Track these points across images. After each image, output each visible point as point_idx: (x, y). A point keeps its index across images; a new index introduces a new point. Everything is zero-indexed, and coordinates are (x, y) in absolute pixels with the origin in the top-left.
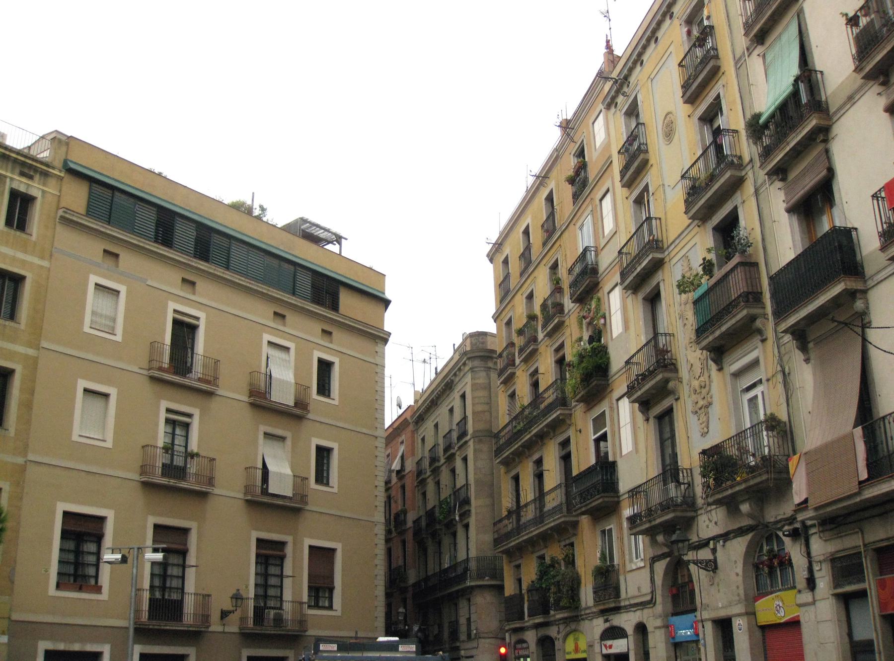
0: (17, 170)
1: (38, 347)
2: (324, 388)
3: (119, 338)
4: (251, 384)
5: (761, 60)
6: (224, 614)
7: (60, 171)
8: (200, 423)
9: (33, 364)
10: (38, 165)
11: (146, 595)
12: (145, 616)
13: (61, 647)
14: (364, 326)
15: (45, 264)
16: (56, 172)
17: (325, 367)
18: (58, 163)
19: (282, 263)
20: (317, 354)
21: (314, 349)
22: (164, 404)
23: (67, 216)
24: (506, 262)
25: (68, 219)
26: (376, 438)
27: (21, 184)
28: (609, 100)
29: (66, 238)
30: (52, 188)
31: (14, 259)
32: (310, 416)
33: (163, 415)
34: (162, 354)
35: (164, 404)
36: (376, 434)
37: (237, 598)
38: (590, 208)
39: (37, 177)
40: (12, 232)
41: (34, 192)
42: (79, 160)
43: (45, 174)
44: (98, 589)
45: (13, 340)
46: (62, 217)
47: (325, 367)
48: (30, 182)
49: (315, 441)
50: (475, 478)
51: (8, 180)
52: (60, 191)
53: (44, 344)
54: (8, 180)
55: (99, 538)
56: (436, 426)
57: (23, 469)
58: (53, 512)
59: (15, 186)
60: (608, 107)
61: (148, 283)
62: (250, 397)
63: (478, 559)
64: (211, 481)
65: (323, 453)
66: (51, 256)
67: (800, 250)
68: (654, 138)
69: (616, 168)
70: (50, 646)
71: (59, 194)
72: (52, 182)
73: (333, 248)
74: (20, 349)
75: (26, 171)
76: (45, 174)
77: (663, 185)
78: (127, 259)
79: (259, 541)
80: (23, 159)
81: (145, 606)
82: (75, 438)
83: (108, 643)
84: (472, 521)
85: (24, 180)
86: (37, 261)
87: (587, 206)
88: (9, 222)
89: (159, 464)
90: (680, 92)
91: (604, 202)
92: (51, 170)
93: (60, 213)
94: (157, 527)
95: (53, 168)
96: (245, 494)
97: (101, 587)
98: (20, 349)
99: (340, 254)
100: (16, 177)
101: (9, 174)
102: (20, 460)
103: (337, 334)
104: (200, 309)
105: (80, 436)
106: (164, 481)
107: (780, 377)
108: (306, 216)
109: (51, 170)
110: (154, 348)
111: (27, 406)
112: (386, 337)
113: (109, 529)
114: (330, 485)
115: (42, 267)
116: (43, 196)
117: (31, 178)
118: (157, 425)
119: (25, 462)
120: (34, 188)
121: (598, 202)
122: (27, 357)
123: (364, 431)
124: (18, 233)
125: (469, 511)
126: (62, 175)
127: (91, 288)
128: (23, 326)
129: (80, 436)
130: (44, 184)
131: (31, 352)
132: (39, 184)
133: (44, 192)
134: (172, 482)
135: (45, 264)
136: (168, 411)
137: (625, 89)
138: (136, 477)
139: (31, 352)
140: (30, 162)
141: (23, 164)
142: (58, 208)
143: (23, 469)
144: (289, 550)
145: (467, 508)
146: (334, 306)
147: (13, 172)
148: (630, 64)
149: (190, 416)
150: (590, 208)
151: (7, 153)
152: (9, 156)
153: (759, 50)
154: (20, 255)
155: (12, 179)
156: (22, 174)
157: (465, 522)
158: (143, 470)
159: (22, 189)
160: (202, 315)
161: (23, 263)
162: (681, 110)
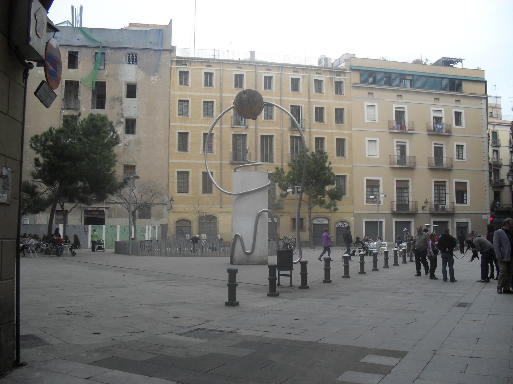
0: (336, 75)
1: (351, 130)
2: (458, 121)
3: (377, 121)
4: (427, 127)
6: (423, 208)
7: (349, 70)
8: (409, 144)
9: (350, 136)
10: (342, 71)
11: (395, 203)
12: (395, 210)
13: (370, 220)
14: (474, 95)
15: (350, 103)
16: (348, 71)
17: (458, 115)
18: (348, 68)
19: (436, 79)
20: (454, 110)
21: (452, 109)
22: (395, 140)
23: (354, 85)
25: (354, 86)
26: (483, 138)
27: (337, 78)
29: (355, 93)
30: (348, 77)
32: (452, 134)
33: (395, 144)
34: (393, 123)
35: (395, 140)
36: (483, 136)
37: (426, 202)
39: (342, 75)
41: (342, 81)
42: (355, 64)
43: (345, 73)
46: (352, 86)
47: (458, 115)
48: (340, 77)
49: (456, 143)
51: (333, 79)
52: (350, 77)
53: (353, 129)
54: (333, 79)
55: (378, 187)
57: (352, 168)
58: (363, 180)
62: (427, 132)
64: (415, 164)
65: (460, 147)
66: (351, 100)
70: (366, 220)
71: (350, 78)
72: (347, 75)
73: (458, 65)
74: (346, 132)
75: (338, 74)
76: (345, 73)
78: (376, 94)
79: (435, 182)
80: (336, 70)
81: (395, 207)
82: (367, 156)
83: (384, 218)
85: (338, 77)
86: (347, 102)
88: (336, 93)
89: (396, 161)
92: (346, 71)
93: (351, 85)
94: (397, 181)
95: (347, 70)
96: (428, 166)
97: (380, 201)
98: (346, 132)
99: (462, 68)
100: (336, 77)
101: (333, 77)
102: (351, 166)
103: (463, 101)
104: (405, 105)
106: (398, 166)
108: (445, 56)
110: (390, 122)
111: (351, 149)
113: (381, 183)
115: (349, 104)
116: (345, 81)
117: (340, 76)
118: (393, 147)
119: (353, 166)
120: (342, 78)
123: (477, 136)
124: (340, 95)
126: (350, 72)
127: (365, 106)
128: (346, 125)
130: (345, 77)
131: (350, 132)
133: (345, 79)
134: (401, 166)
135: (350, 103)
138: (389, 166)
139: (350, 132)
140: (339, 71)
141: (337, 72)
142: (351, 83)
143: (352, 168)
144: (447, 184)
147: (334, 76)
151: (332, 70)
154: (342, 102)
155: (334, 78)
156: (337, 75)
158: (391, 163)
159: (338, 80)
160: (406, 106)
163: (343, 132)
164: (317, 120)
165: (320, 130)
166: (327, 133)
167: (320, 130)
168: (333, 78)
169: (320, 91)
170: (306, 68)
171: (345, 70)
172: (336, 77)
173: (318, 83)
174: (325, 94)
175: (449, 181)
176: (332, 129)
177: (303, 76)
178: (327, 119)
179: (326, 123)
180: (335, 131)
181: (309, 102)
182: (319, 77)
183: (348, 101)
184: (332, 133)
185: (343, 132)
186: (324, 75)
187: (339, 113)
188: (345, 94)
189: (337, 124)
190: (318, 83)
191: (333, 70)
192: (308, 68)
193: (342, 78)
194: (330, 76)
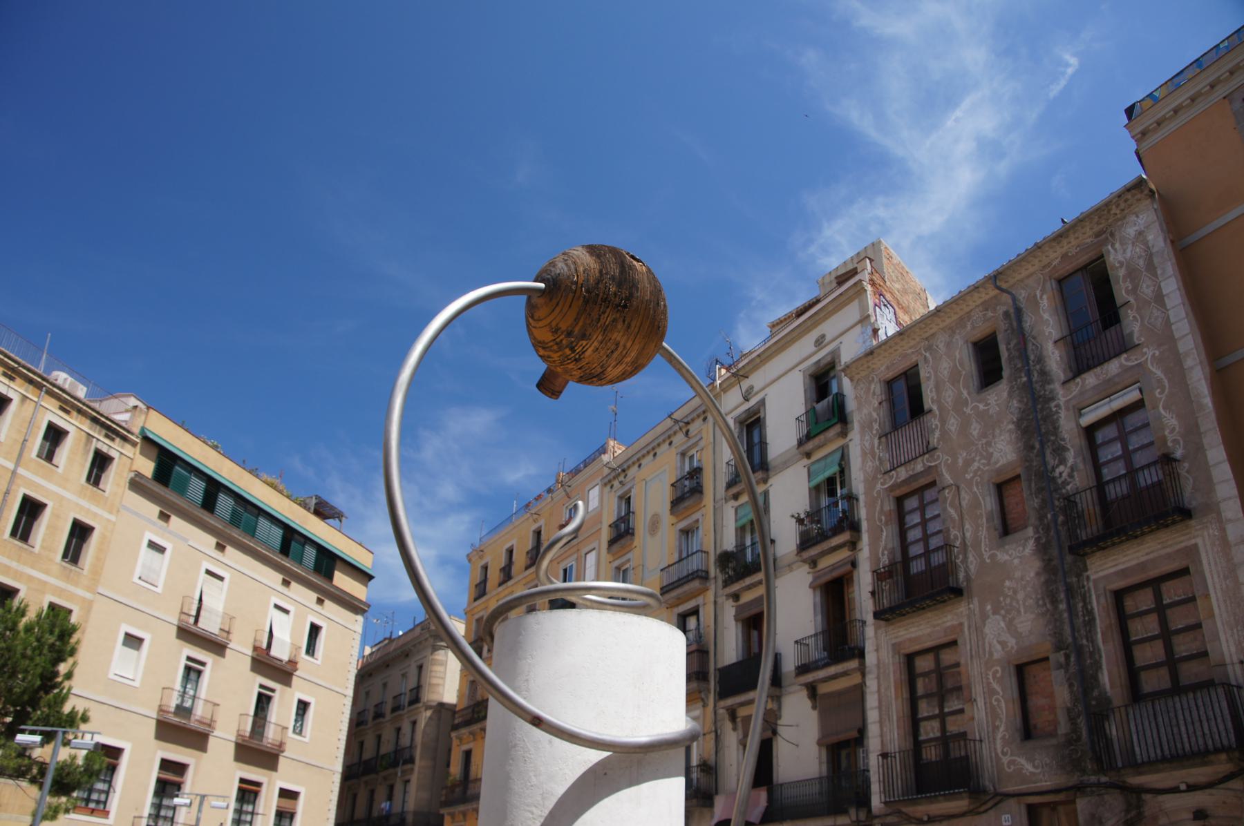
3: (159, 590)
5: (733, 511)
7: (137, 437)
9: (88, 606)
15: (113, 518)
17: (315, 630)
18: (136, 430)
24: (485, 568)
26: (345, 696)
27: (105, 444)
28: (606, 480)
30: (128, 450)
31: (88, 511)
33: (183, 662)
38: (575, 556)
39: (118, 440)
40: (91, 487)
41: (113, 453)
44: (105, 813)
45: (76, 584)
47: (315, 630)
50: (422, 741)
56: (385, 685)
59: (100, 446)
60: (605, 485)
61: (190, 543)
63: (416, 813)
65: (303, 706)
66: (118, 511)
67: (740, 659)
68: (640, 524)
69: (605, 535)
74: (80, 592)
76: (125, 439)
77: (643, 566)
79: (242, 781)
82: (111, 676)
84: (414, 778)
85: (107, 441)
86: (106, 515)
87: (574, 553)
90: (668, 506)
91: (588, 556)
92: (129, 435)
95: (132, 434)
98: (80, 592)
100: (102, 438)
101: (96, 435)
105: (116, 674)
107: (713, 735)
109: (129, 435)
112: (366, 609)
114: (303, 734)
115: (109, 521)
116: (120, 458)
117: (113, 440)
118: (177, 669)
120: (114, 448)
121: (583, 555)
122: (84, 599)
125: (412, 770)
126: (138, 440)
127: (145, 542)
128: (85, 572)
129: (116, 674)
130: (122, 447)
131: (88, 595)
132: (118, 446)
133: (121, 453)
135: (113, 518)
136: (189, 659)
137: (621, 478)
139: (88, 595)
145: (409, 766)
146: (329, 577)
147: (99, 434)
148: (630, 462)
149: (203, 664)
150: (575, 556)
151: (99, 417)
152: (99, 419)
153: (733, 503)
154: (94, 508)
155: (98, 440)
156: (107, 436)
157: (407, 778)
158: (161, 710)
159: (105, 449)
161: (95, 515)
162: (667, 518)
163: (71, 588)
164: (14, 533)
165: (14, 565)
166: (31, 578)
167: (14, 565)
168: (93, 437)
169: (49, 456)
170: (39, 380)
171: (128, 432)
172: (102, 438)
173: (55, 435)
174: (60, 470)
175: (269, 783)
176: (47, 572)
177: (25, 398)
178: (44, 540)
179: (37, 549)
180: (52, 581)
181: (14, 473)
182: (61, 421)
183: (111, 512)
184: (45, 583)
185: (71, 588)
186: (76, 419)
187: (80, 532)
188: (108, 491)
189: (64, 564)
190: (55, 435)
191: (103, 419)
192: (45, 383)
193: (114, 448)
194: (91, 429)
